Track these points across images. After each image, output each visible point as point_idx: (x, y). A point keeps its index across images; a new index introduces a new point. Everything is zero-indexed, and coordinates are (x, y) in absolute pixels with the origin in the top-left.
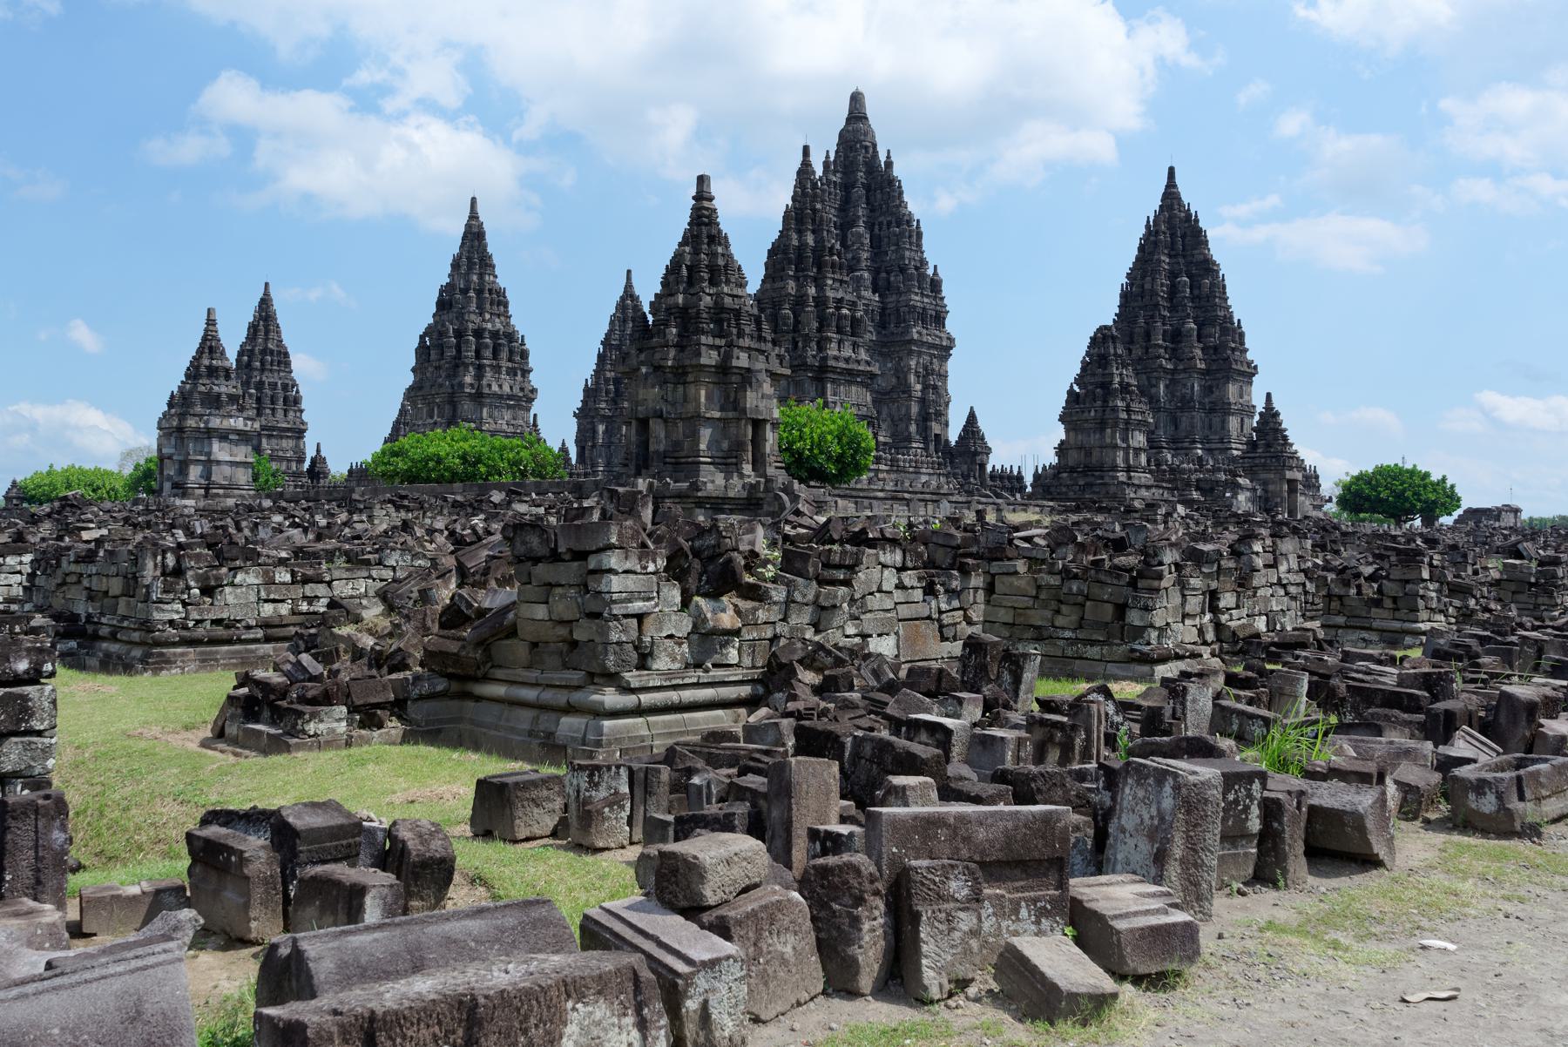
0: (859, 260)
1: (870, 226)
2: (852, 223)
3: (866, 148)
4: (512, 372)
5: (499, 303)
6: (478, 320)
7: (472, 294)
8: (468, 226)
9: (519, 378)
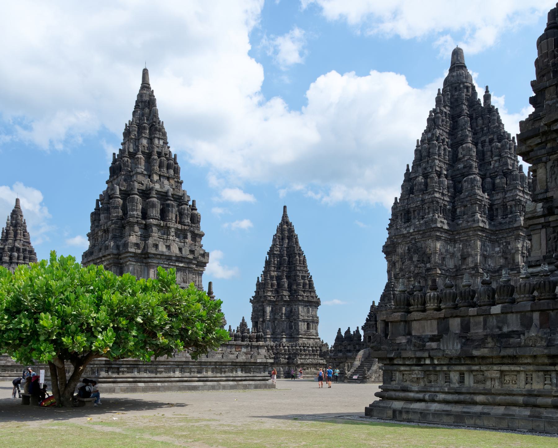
0: (471, 167)
1: (476, 144)
2: (463, 141)
3: (467, 88)
4: (181, 234)
5: (169, 167)
6: (146, 181)
7: (140, 156)
8: (140, 95)
9: (189, 240)
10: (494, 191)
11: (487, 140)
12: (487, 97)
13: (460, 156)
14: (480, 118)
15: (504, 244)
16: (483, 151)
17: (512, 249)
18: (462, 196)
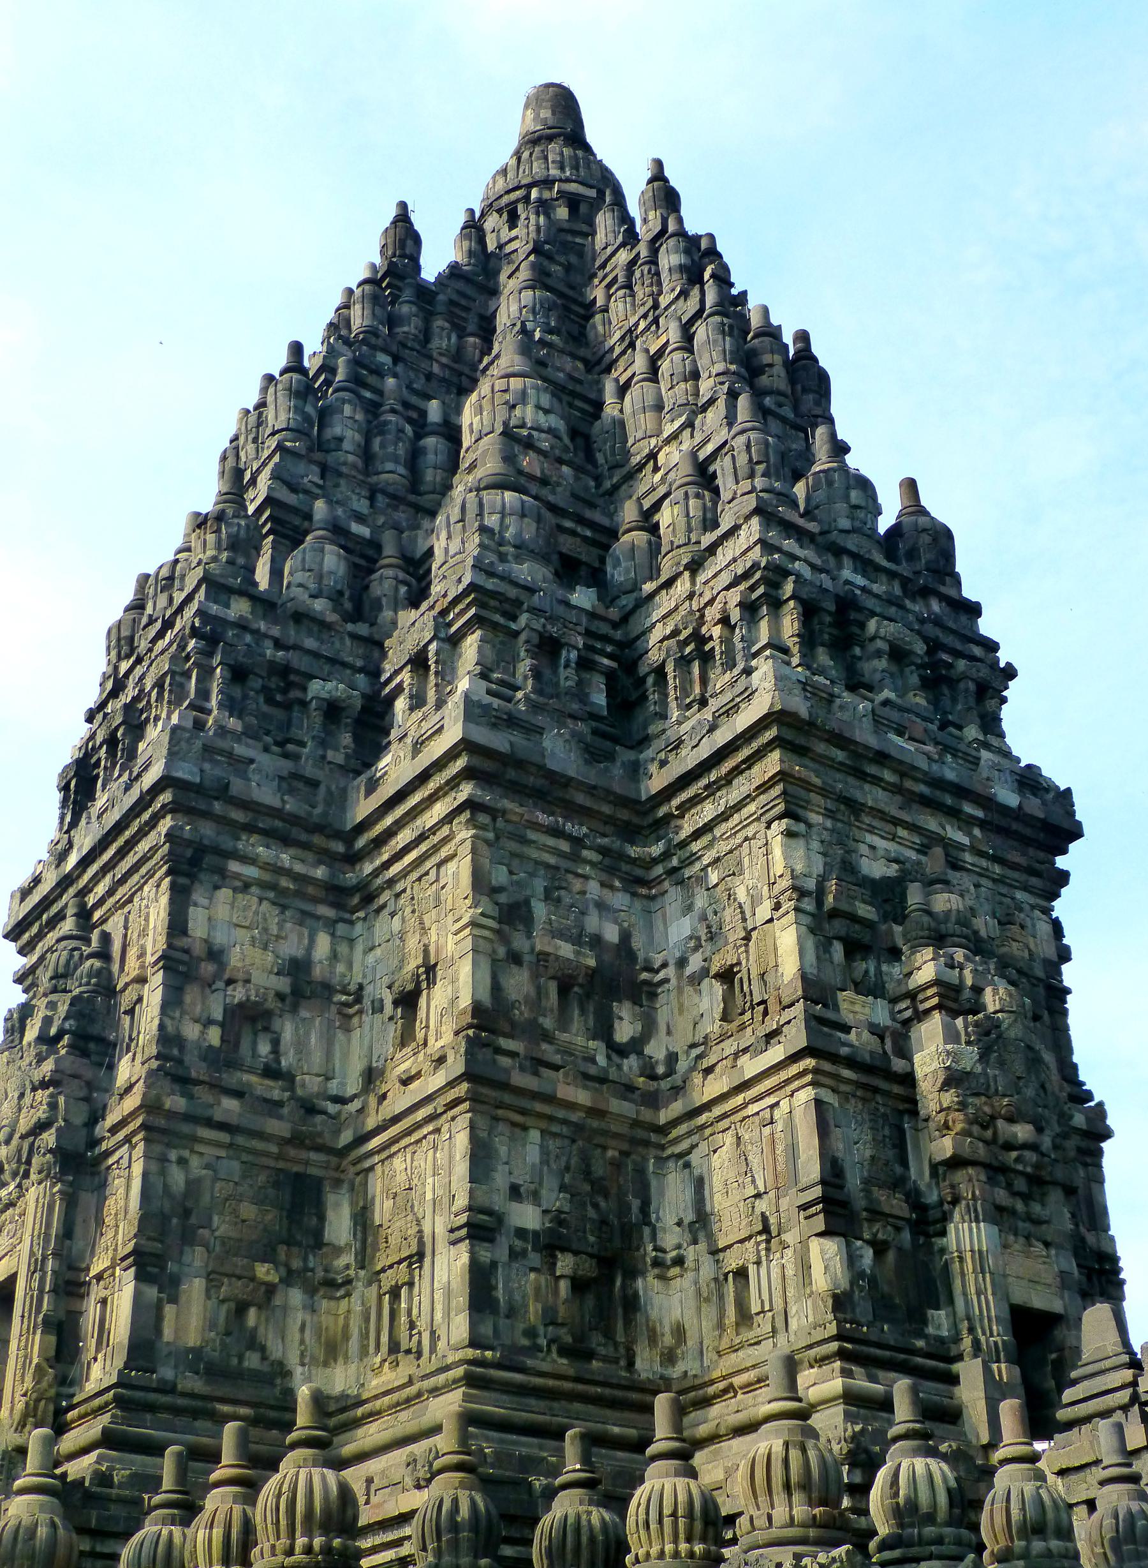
12: (666, 198)
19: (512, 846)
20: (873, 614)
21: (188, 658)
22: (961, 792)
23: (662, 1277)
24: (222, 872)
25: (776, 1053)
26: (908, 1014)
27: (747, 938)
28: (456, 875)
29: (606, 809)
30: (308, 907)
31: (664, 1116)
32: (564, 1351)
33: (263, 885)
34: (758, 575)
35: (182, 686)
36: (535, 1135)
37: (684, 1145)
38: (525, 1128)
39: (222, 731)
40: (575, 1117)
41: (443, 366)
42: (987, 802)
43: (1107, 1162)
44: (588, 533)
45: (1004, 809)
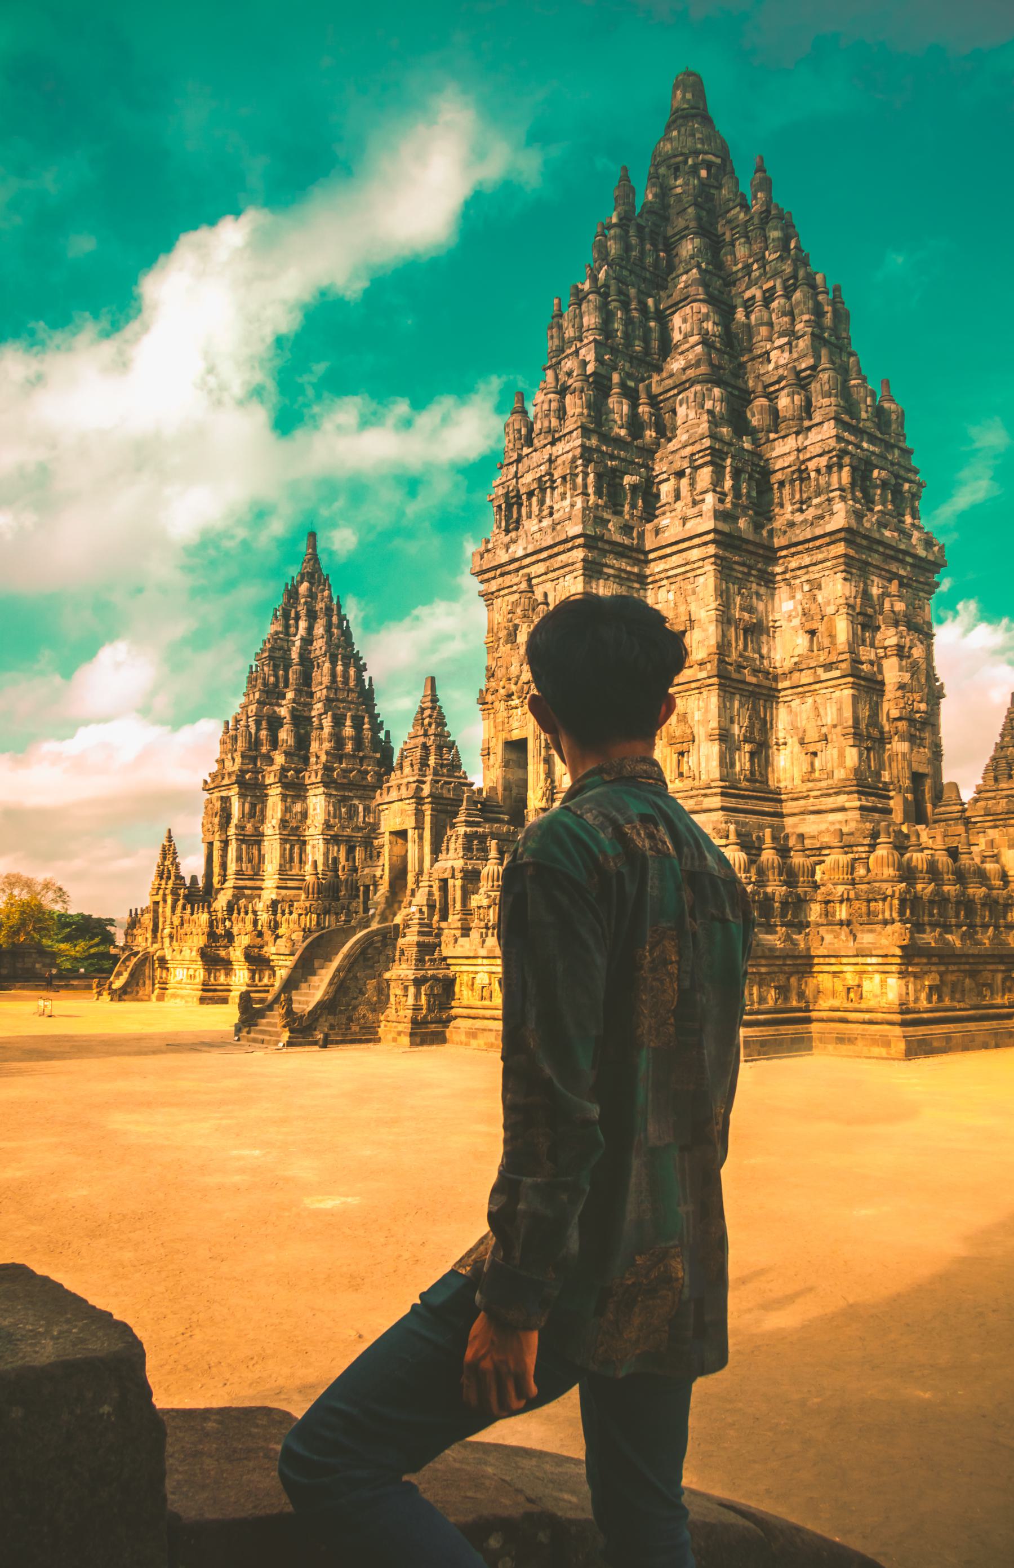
10: (777, 432)
11: (759, 294)
13: (677, 337)
14: (742, 240)
15: (806, 588)
16: (748, 326)
17: (828, 603)
18: (672, 446)
19: (727, 571)
20: (877, 467)
21: (577, 467)
22: (906, 553)
23: (778, 750)
24: (601, 573)
25: (837, 673)
26: (883, 654)
27: (822, 619)
28: (706, 585)
29: (761, 552)
30: (630, 584)
31: (780, 686)
32: (748, 780)
33: (614, 576)
34: (834, 453)
35: (574, 481)
36: (738, 697)
37: (788, 699)
38: (734, 694)
39: (597, 506)
40: (751, 688)
41: (651, 272)
42: (915, 556)
43: (942, 706)
44: (737, 393)
45: (921, 559)
